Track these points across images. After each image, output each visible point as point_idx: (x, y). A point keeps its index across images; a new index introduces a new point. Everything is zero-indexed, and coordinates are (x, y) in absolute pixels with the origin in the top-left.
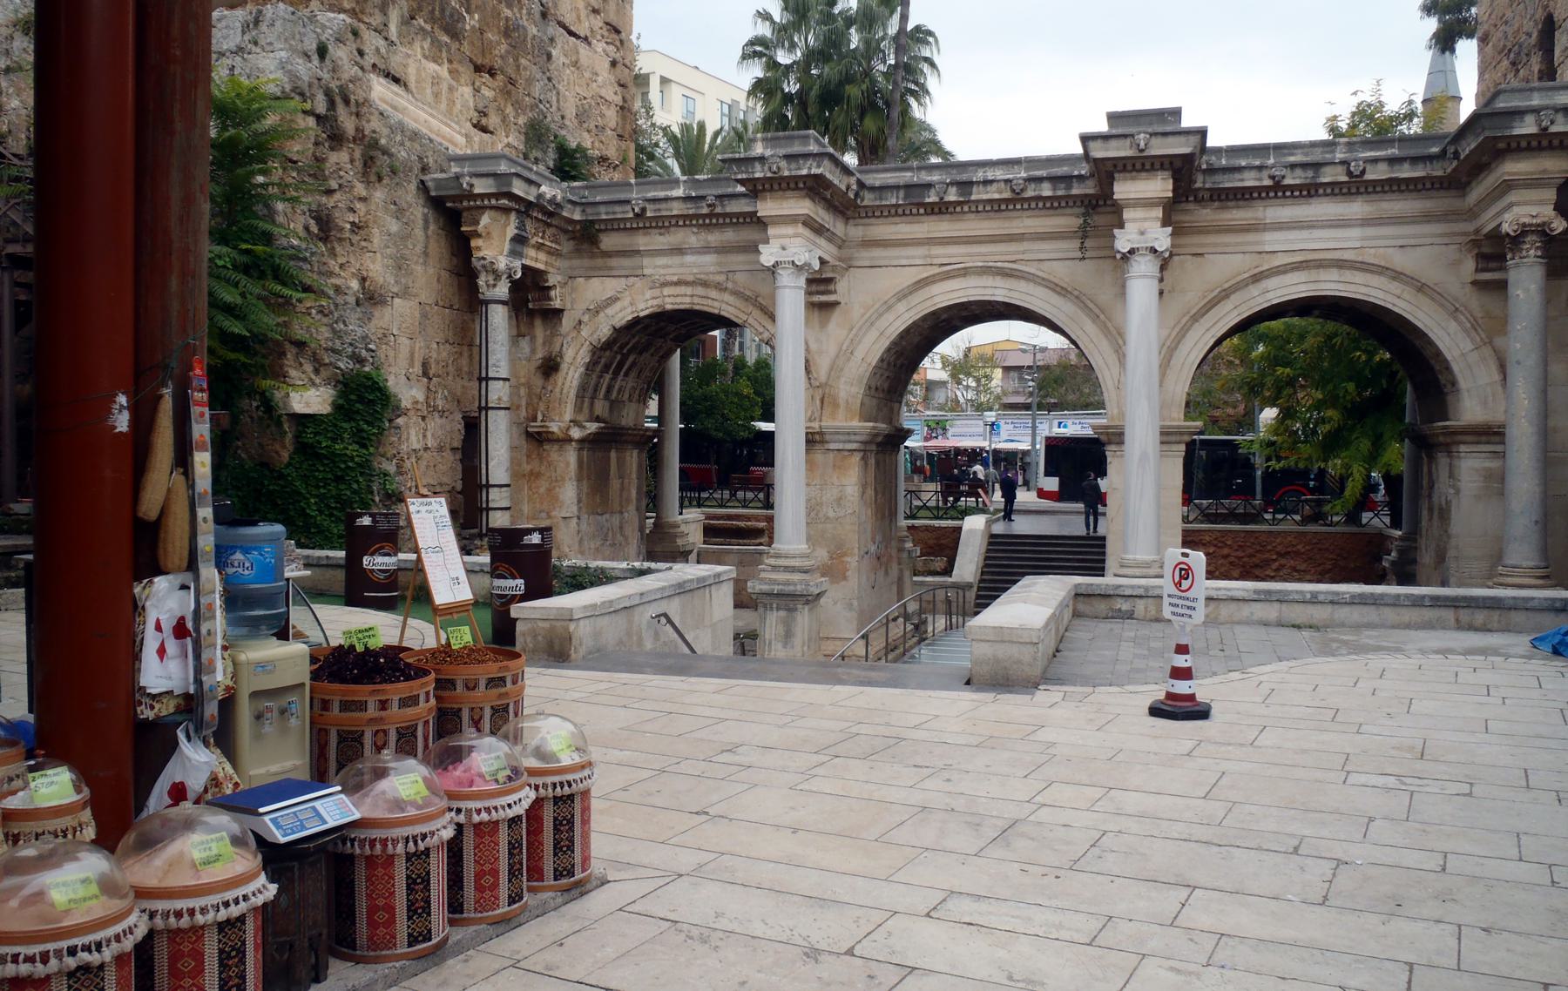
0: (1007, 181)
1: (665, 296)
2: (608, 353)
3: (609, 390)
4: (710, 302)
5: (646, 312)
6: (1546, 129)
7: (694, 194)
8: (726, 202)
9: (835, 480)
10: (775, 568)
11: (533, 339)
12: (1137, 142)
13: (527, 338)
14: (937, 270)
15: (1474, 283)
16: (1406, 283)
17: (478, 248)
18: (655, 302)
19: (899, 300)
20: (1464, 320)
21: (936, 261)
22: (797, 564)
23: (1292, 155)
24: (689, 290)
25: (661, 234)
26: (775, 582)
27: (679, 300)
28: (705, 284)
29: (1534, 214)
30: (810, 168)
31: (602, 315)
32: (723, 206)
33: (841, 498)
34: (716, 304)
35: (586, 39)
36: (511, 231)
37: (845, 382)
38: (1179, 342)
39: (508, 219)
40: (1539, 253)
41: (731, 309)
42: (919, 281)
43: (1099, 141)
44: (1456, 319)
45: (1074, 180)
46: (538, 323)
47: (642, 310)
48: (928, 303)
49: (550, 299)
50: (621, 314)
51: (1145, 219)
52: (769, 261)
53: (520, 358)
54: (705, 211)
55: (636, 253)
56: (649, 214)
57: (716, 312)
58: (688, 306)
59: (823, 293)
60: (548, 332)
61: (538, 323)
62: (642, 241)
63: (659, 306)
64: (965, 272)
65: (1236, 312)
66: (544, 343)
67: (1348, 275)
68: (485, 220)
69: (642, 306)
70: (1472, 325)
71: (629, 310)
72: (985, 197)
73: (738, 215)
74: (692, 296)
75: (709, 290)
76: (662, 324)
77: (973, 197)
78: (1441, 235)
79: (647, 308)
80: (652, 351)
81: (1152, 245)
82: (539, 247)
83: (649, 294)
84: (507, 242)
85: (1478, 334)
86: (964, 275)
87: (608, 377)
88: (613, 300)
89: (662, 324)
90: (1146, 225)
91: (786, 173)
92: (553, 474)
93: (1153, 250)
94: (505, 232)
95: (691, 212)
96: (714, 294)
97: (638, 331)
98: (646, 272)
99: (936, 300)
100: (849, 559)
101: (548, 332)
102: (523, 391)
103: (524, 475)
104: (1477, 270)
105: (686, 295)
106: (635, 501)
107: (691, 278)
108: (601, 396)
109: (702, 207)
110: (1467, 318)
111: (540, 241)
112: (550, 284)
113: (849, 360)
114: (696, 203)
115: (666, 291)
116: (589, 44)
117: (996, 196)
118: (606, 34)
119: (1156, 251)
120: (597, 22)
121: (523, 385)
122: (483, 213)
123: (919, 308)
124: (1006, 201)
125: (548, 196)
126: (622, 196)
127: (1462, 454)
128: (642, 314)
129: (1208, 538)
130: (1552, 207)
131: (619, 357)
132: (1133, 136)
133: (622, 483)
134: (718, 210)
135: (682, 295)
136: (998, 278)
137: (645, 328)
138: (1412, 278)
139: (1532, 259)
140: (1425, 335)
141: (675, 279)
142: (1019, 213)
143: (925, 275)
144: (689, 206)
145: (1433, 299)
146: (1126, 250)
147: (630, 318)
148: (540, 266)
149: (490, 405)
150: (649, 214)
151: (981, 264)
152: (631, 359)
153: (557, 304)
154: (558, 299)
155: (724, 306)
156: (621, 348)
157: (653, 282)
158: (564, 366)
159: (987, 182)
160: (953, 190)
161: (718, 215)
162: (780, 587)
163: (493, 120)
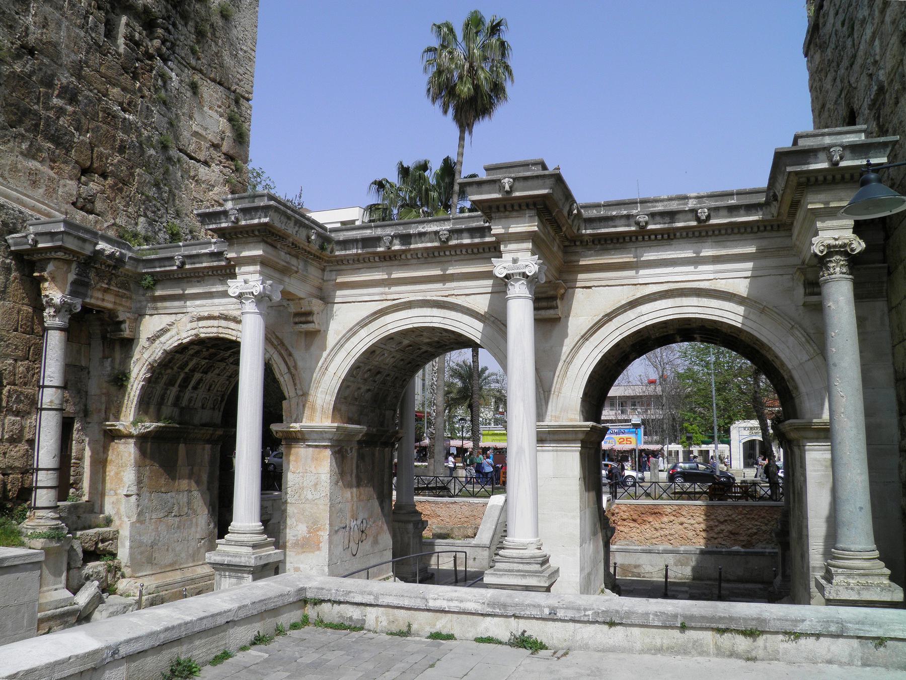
2: (169, 371)
3: (178, 398)
4: (230, 331)
5: (187, 340)
6: (837, 164)
9: (313, 469)
10: (229, 543)
11: (113, 362)
13: (109, 360)
17: (45, 289)
18: (193, 332)
19: (362, 327)
21: (389, 297)
22: (246, 539)
23: (655, 207)
26: (227, 554)
27: (209, 330)
28: (226, 318)
29: (836, 237)
31: (158, 342)
33: (316, 485)
34: (234, 333)
35: (206, 163)
36: (72, 277)
37: (322, 391)
38: (573, 357)
39: (70, 267)
40: (844, 270)
42: (375, 313)
43: (474, 186)
44: (793, 335)
46: (117, 348)
48: (383, 329)
49: (122, 331)
50: (170, 342)
51: (518, 250)
52: (234, 293)
53: (103, 375)
56: (187, 267)
57: (234, 338)
60: (123, 356)
61: (117, 348)
63: (197, 335)
64: (409, 305)
65: (618, 332)
66: (120, 364)
67: (705, 301)
68: (50, 267)
69: (184, 335)
70: (806, 339)
71: (176, 338)
76: (212, 351)
78: (776, 267)
80: (217, 371)
81: (523, 271)
82: (106, 291)
83: (190, 326)
84: (69, 284)
85: (812, 346)
86: (410, 308)
87: (174, 391)
88: (164, 331)
89: (212, 351)
90: (519, 255)
92: (121, 462)
93: (524, 275)
94: (67, 277)
97: (193, 355)
98: (189, 310)
100: (320, 533)
101: (123, 356)
102: (104, 399)
103: (100, 462)
104: (806, 294)
106: (206, 482)
107: (216, 314)
108: (169, 403)
110: (801, 333)
111: (106, 286)
112: (121, 318)
113: (324, 374)
114: (218, 257)
115: (202, 323)
116: (209, 166)
118: (224, 161)
119: (528, 276)
120: (215, 154)
121: (103, 394)
122: (49, 263)
123: (377, 333)
125: (107, 253)
126: (169, 255)
128: (185, 341)
129: (669, 511)
130: (851, 230)
131: (182, 375)
132: (500, 180)
133: (192, 469)
137: (197, 353)
138: (755, 302)
139: (838, 275)
140: (770, 348)
141: (206, 314)
142: (449, 258)
146: (502, 276)
147: (176, 344)
148: (109, 306)
149: (43, 407)
152: (197, 376)
153: (127, 334)
154: (128, 330)
156: (182, 368)
158: (132, 380)
159: (421, 235)
160: (396, 241)
162: (229, 558)
163: (99, 206)
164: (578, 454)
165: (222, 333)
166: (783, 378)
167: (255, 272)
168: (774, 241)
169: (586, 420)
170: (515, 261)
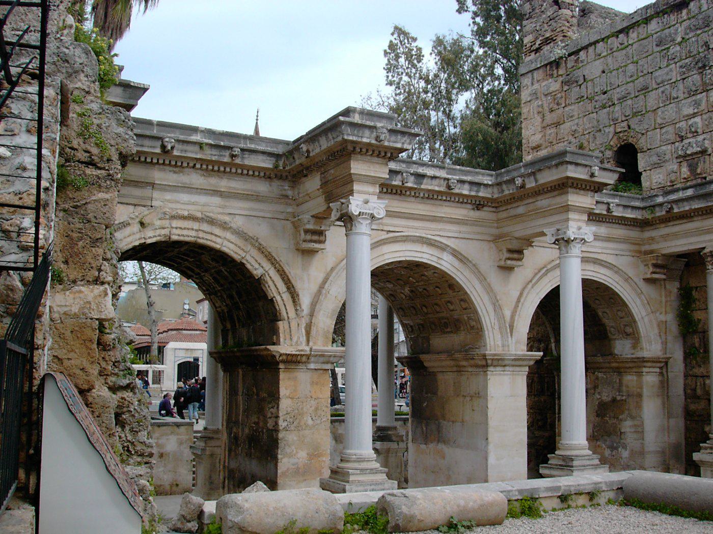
0: (445, 179)
1: (172, 228)
4: (213, 238)
7: (222, 144)
8: (246, 156)
12: (593, 171)
14: (384, 236)
15: (647, 280)
16: (620, 276)
18: (163, 232)
20: (644, 299)
21: (386, 228)
24: (196, 225)
25: (175, 172)
27: (185, 232)
28: (212, 222)
30: (403, 143)
32: (243, 158)
34: (219, 240)
41: (232, 246)
45: (482, 187)
47: (150, 238)
48: (381, 259)
54: (227, 159)
55: (153, 185)
57: (218, 247)
58: (192, 239)
59: (315, 242)
62: (159, 176)
71: (138, 236)
72: (430, 188)
73: (254, 169)
74: (197, 231)
75: (214, 227)
77: (423, 187)
78: (630, 251)
79: (155, 236)
86: (404, 241)
91: (386, 144)
95: (214, 158)
96: (217, 231)
99: (386, 257)
105: (193, 229)
109: (225, 156)
110: (646, 298)
115: (175, 223)
117: (437, 189)
124: (439, 192)
127: (644, 373)
128: (149, 241)
134: (238, 161)
135: (188, 229)
136: (425, 246)
141: (186, 213)
143: (383, 237)
144: (214, 153)
145: (631, 286)
147: (137, 243)
150: (176, 153)
151: (418, 235)
155: (226, 243)
157: (165, 213)
160: (412, 178)
161: (238, 166)
164: (526, 377)
165: (203, 238)
166: (603, 325)
167: (373, 194)
168: (634, 234)
169: (530, 349)
170: (579, 228)
